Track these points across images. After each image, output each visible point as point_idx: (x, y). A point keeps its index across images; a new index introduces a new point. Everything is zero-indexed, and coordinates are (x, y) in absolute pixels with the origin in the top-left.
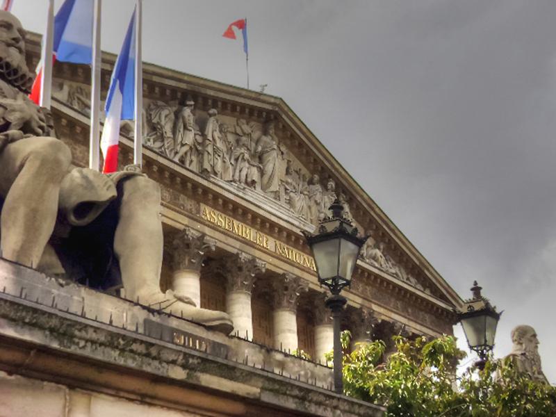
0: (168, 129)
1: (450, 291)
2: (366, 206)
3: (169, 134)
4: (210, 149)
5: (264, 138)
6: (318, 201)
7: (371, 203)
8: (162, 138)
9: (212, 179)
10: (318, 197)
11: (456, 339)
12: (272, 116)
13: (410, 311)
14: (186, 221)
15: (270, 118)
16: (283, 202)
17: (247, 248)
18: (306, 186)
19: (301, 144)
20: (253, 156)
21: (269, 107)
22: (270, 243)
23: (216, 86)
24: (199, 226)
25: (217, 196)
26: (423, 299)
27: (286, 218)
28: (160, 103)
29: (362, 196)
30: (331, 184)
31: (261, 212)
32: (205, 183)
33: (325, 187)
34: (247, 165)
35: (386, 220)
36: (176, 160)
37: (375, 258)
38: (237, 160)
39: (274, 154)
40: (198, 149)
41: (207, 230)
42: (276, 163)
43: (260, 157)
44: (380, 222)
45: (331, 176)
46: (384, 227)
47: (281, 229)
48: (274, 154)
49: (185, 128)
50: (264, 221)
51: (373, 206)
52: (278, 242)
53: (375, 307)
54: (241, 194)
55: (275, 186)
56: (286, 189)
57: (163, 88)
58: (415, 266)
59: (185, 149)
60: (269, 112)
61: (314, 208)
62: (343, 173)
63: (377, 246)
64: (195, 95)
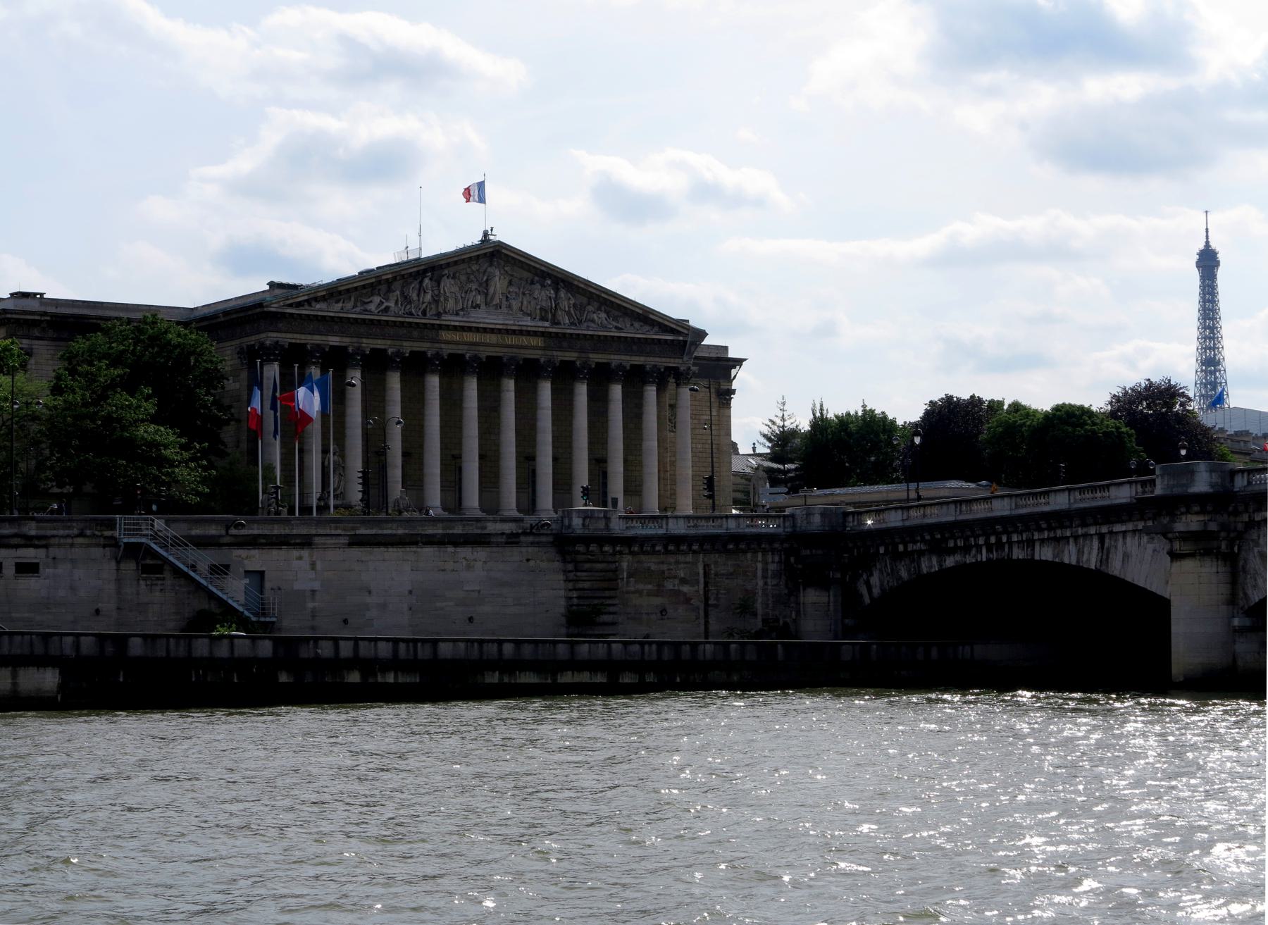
0: (414, 297)
3: (415, 298)
5: (489, 269)
7: (588, 283)
8: (410, 302)
10: (536, 294)
13: (635, 348)
14: (428, 345)
16: (504, 309)
20: (480, 285)
22: (493, 339)
33: (543, 286)
39: (497, 279)
40: (436, 301)
42: (499, 284)
45: (549, 276)
47: (500, 330)
48: (497, 279)
53: (591, 356)
55: (496, 301)
61: (533, 302)
63: (599, 309)
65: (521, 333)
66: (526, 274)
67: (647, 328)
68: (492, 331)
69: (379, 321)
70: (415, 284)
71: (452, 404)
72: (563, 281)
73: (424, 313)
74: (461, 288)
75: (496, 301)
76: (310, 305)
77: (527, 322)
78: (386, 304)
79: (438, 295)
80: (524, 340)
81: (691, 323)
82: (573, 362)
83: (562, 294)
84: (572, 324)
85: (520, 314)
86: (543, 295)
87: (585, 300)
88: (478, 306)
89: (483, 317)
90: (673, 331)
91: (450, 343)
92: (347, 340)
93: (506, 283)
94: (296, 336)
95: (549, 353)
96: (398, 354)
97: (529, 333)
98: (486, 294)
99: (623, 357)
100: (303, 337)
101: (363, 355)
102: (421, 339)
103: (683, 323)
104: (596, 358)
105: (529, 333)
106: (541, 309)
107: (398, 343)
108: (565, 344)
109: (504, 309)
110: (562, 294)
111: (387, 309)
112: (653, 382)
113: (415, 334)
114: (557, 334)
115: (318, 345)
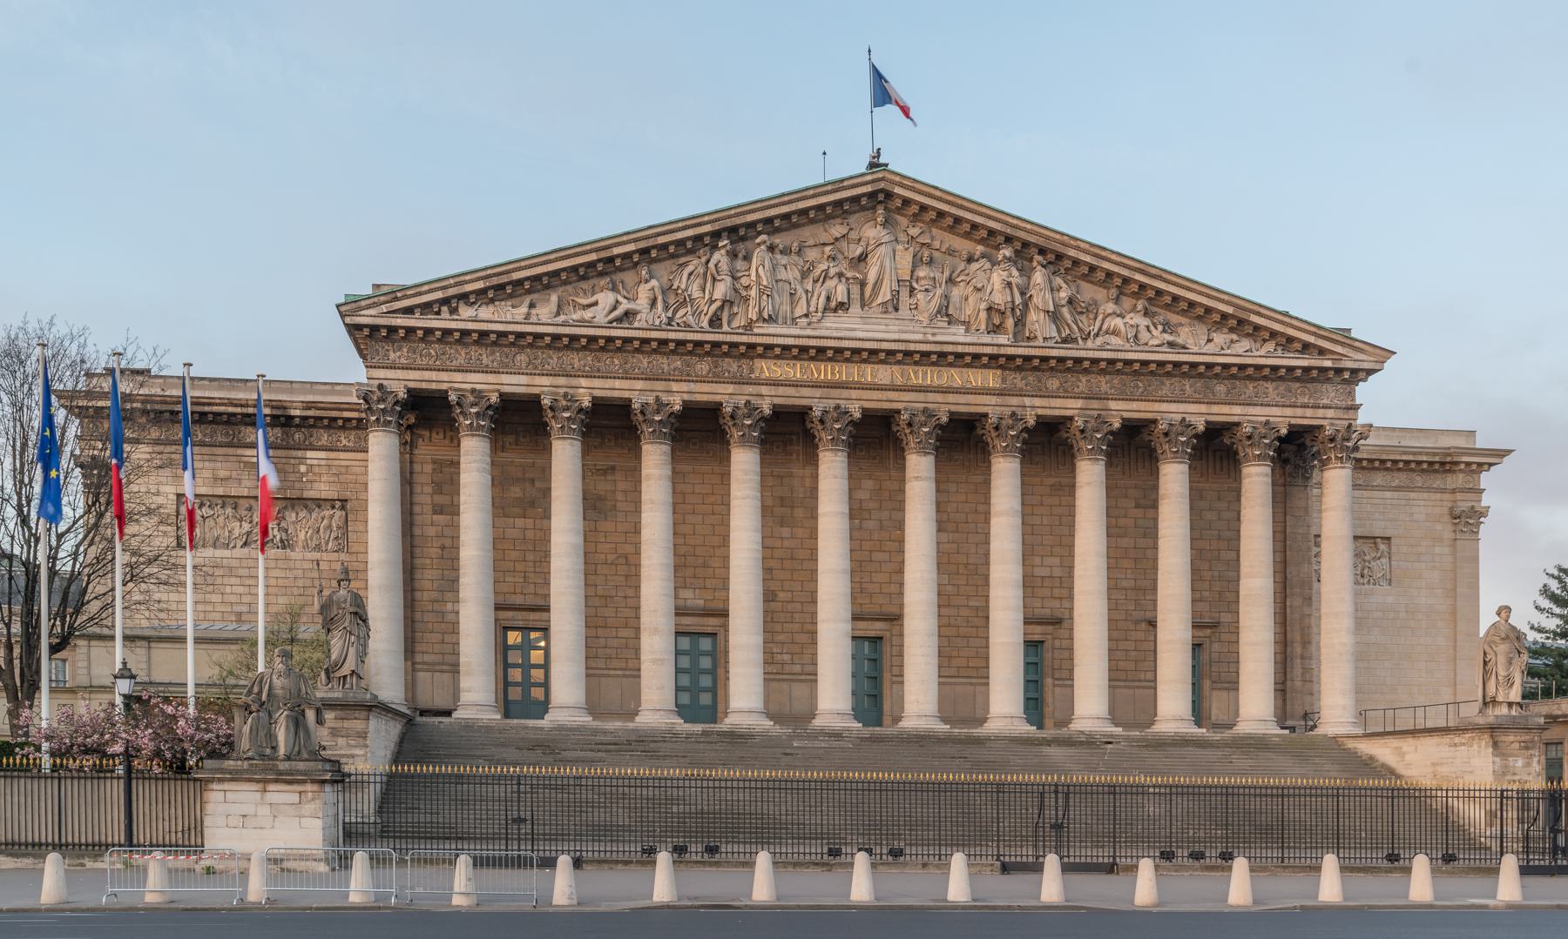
2: (1088, 259)
4: (753, 293)
9: (756, 331)
11: (1356, 408)
12: (881, 197)
13: (1221, 389)
14: (730, 388)
15: (879, 197)
18: (962, 266)
21: (868, 189)
27: (896, 336)
28: (682, 260)
29: (1077, 248)
32: (744, 339)
33: (994, 263)
34: (836, 280)
36: (705, 324)
37: (1115, 333)
38: (816, 281)
41: (764, 390)
43: (863, 258)
44: (1125, 272)
45: (1009, 239)
47: (890, 353)
49: (714, 279)
52: (895, 368)
53: (1113, 405)
54: (809, 332)
56: (912, 290)
57: (680, 243)
58: (1225, 316)
59: (714, 307)
60: (872, 195)
63: (1134, 309)
64: (733, 230)
65: (941, 358)
67: (1246, 344)
68: (873, 356)
69: (610, 340)
70: (694, 264)
71: (788, 514)
72: (1042, 251)
73: (715, 321)
74: (804, 275)
75: (885, 295)
76: (454, 311)
78: (625, 306)
79: (747, 288)
80: (955, 377)
81: (1353, 335)
82: (1071, 418)
83: (1039, 276)
84: (1065, 341)
85: (942, 322)
86: (997, 281)
87: (1100, 294)
88: (841, 306)
89: (854, 328)
90: (1306, 347)
92: (545, 381)
93: (905, 260)
94: (433, 375)
95: (1015, 401)
97: (959, 359)
98: (863, 284)
100: (444, 376)
101: (581, 410)
102: (717, 379)
103: (1343, 336)
104: (1121, 410)
105: (959, 359)
106: (989, 309)
107: (659, 385)
108: (1053, 383)
109: (904, 312)
110: (1039, 276)
111: (629, 315)
113: (703, 367)
115: (473, 391)
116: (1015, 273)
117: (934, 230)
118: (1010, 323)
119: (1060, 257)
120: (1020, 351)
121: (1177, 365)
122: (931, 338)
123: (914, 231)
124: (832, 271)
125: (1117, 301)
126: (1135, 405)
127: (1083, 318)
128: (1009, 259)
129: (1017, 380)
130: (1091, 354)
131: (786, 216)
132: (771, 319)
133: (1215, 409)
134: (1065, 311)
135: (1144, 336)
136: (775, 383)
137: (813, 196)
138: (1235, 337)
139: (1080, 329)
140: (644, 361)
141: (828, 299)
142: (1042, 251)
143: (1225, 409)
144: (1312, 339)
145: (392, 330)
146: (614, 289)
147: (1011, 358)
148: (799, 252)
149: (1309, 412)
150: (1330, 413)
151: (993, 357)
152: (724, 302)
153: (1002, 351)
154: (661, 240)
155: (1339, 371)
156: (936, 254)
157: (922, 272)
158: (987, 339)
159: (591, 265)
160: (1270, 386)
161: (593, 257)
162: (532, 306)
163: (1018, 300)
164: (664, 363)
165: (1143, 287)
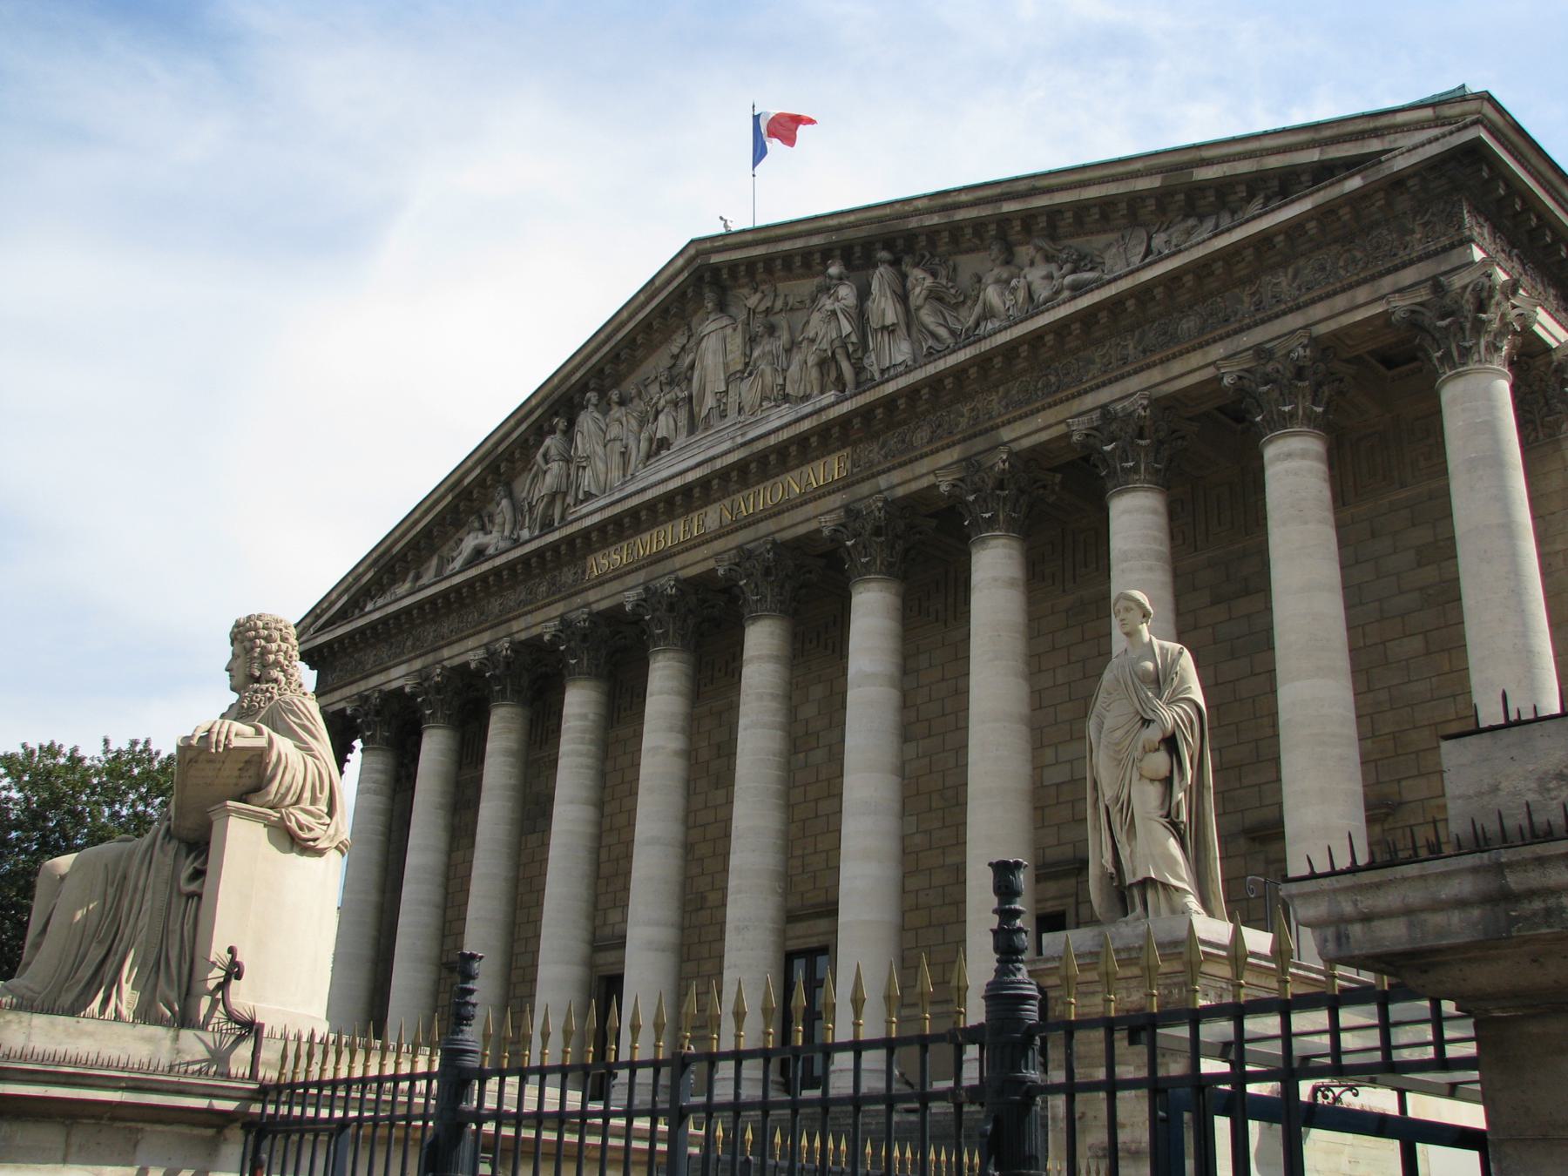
1: (1327, 133)
2: (936, 219)
6: (812, 335)
7: (942, 201)
12: (707, 276)
13: (1188, 324)
17: (659, 569)
19: (768, 260)
21: (686, 274)
23: (578, 359)
24: (578, 600)
25: (586, 533)
26: (1202, 268)
29: (918, 213)
30: (834, 270)
31: (649, 495)
32: (556, 536)
35: (998, 190)
41: (591, 596)
46: (1009, 207)
47: (704, 483)
48: (711, 345)
50: (669, 498)
51: (949, 200)
53: (1006, 434)
54: (617, 496)
62: (852, 218)
63: (1032, 264)
66: (806, 286)
67: (1209, 224)
74: (642, 423)
76: (362, 609)
77: (777, 422)
80: (793, 483)
88: (664, 444)
91: (614, 580)
92: (418, 664)
95: (865, 488)
96: (492, 655)
99: (1134, 383)
101: (438, 688)
106: (822, 364)
108: (921, 436)
111: (479, 554)
112: (1282, 423)
114: (866, 412)
116: (846, 293)
117: (780, 286)
118: (846, 366)
119: (911, 237)
120: (846, 407)
121: (1087, 317)
122: (739, 440)
123: (753, 301)
124: (662, 402)
125: (1007, 262)
126: (1039, 420)
127: (963, 312)
128: (840, 278)
129: (873, 452)
130: (941, 365)
131: (615, 357)
132: (589, 496)
133: (1177, 367)
134: (927, 317)
135: (1043, 292)
136: (601, 581)
137: (631, 318)
138: (1191, 222)
139: (952, 332)
140: (495, 606)
141: (651, 440)
142: (888, 244)
143: (1195, 359)
144: (1314, 155)
145: (320, 648)
146: (483, 528)
147: (844, 421)
148: (639, 394)
149: (1362, 294)
150: (1408, 276)
151: (824, 431)
152: (553, 497)
153: (824, 417)
154: (500, 449)
155: (1397, 182)
156: (773, 319)
157: (756, 354)
158: (807, 408)
159: (453, 508)
160: (1283, 280)
161: (450, 498)
162: (418, 577)
163: (847, 328)
164: (512, 598)
165: (1028, 218)
